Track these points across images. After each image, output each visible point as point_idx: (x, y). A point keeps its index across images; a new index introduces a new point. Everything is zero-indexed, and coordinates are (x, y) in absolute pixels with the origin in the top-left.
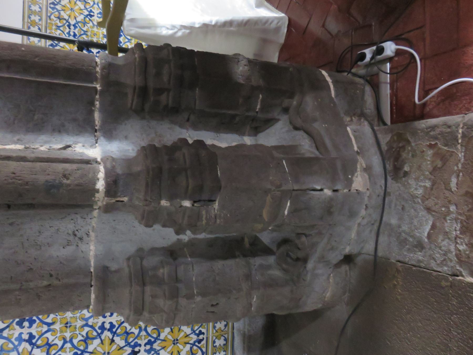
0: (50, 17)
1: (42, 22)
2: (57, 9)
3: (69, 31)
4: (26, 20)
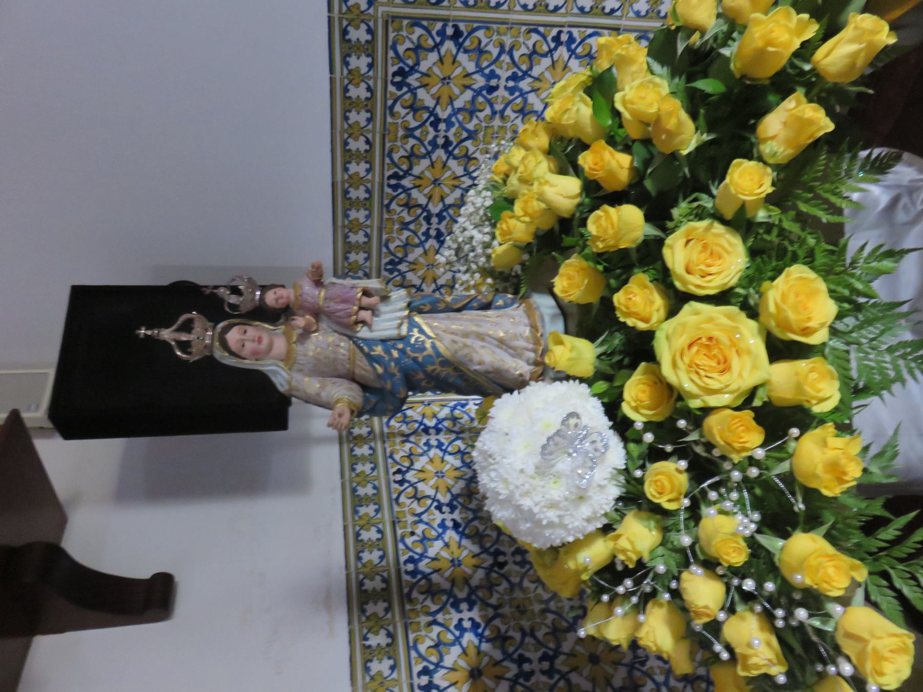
0: (388, 206)
1: (372, 222)
2: (403, 187)
3: (428, 229)
4: (340, 223)
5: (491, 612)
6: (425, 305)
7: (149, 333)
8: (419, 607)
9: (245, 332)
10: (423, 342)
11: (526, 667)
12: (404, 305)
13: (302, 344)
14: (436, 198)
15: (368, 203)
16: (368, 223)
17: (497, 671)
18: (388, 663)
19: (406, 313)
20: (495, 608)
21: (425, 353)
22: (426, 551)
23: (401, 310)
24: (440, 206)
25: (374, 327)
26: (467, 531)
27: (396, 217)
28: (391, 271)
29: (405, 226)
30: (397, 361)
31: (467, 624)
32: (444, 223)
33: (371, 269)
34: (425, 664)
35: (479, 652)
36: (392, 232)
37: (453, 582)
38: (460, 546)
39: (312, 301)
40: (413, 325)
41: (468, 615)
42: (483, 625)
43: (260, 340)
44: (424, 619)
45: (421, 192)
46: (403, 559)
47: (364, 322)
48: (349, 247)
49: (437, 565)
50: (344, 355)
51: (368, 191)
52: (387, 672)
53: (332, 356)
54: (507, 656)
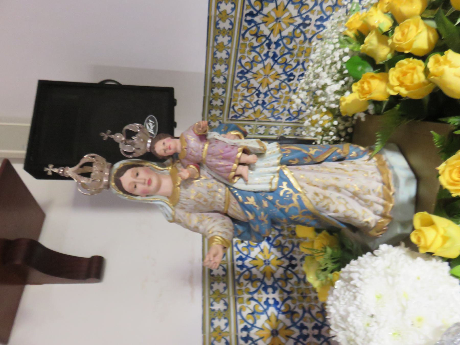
0: (243, 35)
1: (232, 45)
2: (255, 22)
3: (268, 52)
5: (286, 295)
6: (294, 160)
7: (56, 170)
8: (243, 288)
9: (137, 175)
10: (291, 195)
11: (305, 332)
12: (278, 161)
13: (186, 188)
14: (276, 31)
15: (230, 32)
16: (230, 45)
17: (287, 332)
18: (224, 321)
19: (278, 168)
20: (289, 293)
21: (291, 205)
22: (249, 253)
23: (274, 166)
24: (278, 37)
25: (249, 182)
26: (274, 243)
27: (248, 43)
28: (241, 78)
29: (253, 49)
30: (266, 211)
31: (271, 302)
32: (279, 48)
33: (228, 76)
34: (245, 324)
35: (277, 320)
36: (244, 52)
37: (264, 274)
38: (270, 252)
39: (196, 154)
40: (283, 178)
41: (273, 296)
42: (280, 303)
43: (150, 182)
44: (246, 296)
45: (266, 26)
46: (236, 257)
47: (240, 176)
48: (216, 61)
49: (256, 263)
50: (221, 199)
51: (231, 24)
52: (223, 327)
53: (210, 200)
54: (294, 324)
